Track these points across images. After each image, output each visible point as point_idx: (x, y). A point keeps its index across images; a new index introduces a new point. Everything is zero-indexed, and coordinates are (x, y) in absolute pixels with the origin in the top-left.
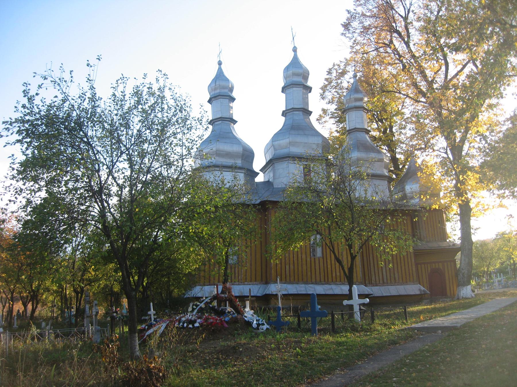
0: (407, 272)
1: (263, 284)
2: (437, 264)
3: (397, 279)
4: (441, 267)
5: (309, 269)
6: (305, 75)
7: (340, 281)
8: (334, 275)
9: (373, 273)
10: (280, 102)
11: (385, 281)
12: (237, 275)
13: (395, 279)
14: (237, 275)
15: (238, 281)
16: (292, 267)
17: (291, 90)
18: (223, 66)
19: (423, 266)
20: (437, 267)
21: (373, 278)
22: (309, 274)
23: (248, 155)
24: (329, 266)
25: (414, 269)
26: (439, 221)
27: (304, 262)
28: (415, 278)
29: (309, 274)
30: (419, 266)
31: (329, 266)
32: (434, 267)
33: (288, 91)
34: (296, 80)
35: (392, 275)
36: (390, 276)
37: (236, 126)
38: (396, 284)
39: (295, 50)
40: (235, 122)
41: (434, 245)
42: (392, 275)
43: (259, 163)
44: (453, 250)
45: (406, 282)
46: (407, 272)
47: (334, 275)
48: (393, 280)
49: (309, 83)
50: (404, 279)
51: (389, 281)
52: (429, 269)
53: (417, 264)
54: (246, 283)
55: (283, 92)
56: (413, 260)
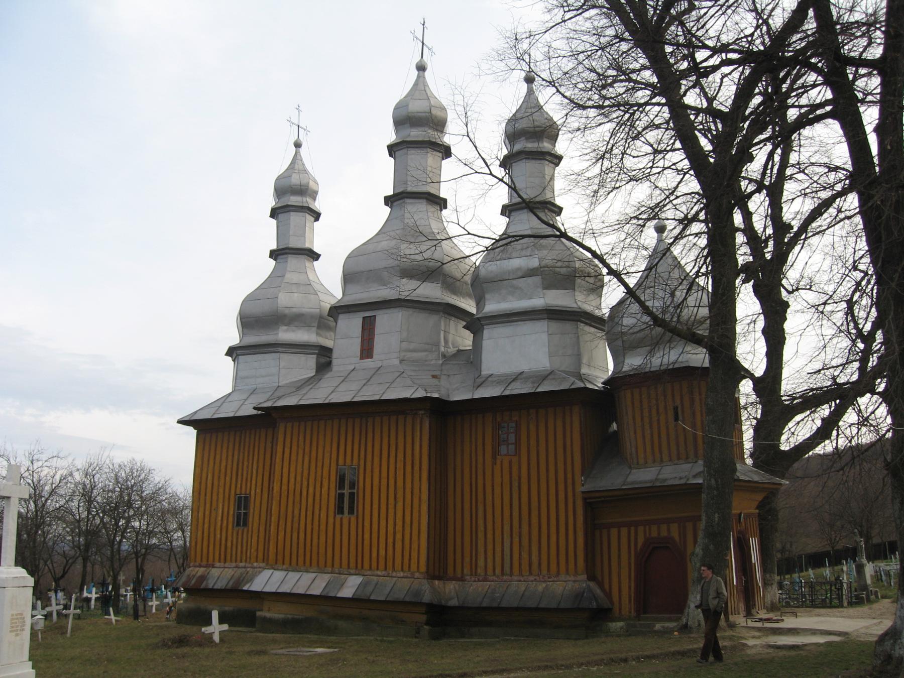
2: (664, 527)
3: (535, 566)
4: (675, 534)
5: (330, 541)
7: (386, 569)
8: (374, 555)
12: (244, 548)
13: (530, 565)
14: (244, 548)
15: (246, 561)
18: (303, 150)
19: (624, 531)
20: (664, 533)
21: (481, 563)
24: (367, 536)
26: (676, 409)
31: (367, 536)
32: (654, 534)
34: (419, 133)
35: (525, 555)
36: (520, 559)
38: (532, 578)
39: (421, 68)
42: (525, 555)
45: (558, 573)
47: (374, 555)
48: (525, 566)
50: (553, 566)
52: (641, 541)
54: (255, 564)
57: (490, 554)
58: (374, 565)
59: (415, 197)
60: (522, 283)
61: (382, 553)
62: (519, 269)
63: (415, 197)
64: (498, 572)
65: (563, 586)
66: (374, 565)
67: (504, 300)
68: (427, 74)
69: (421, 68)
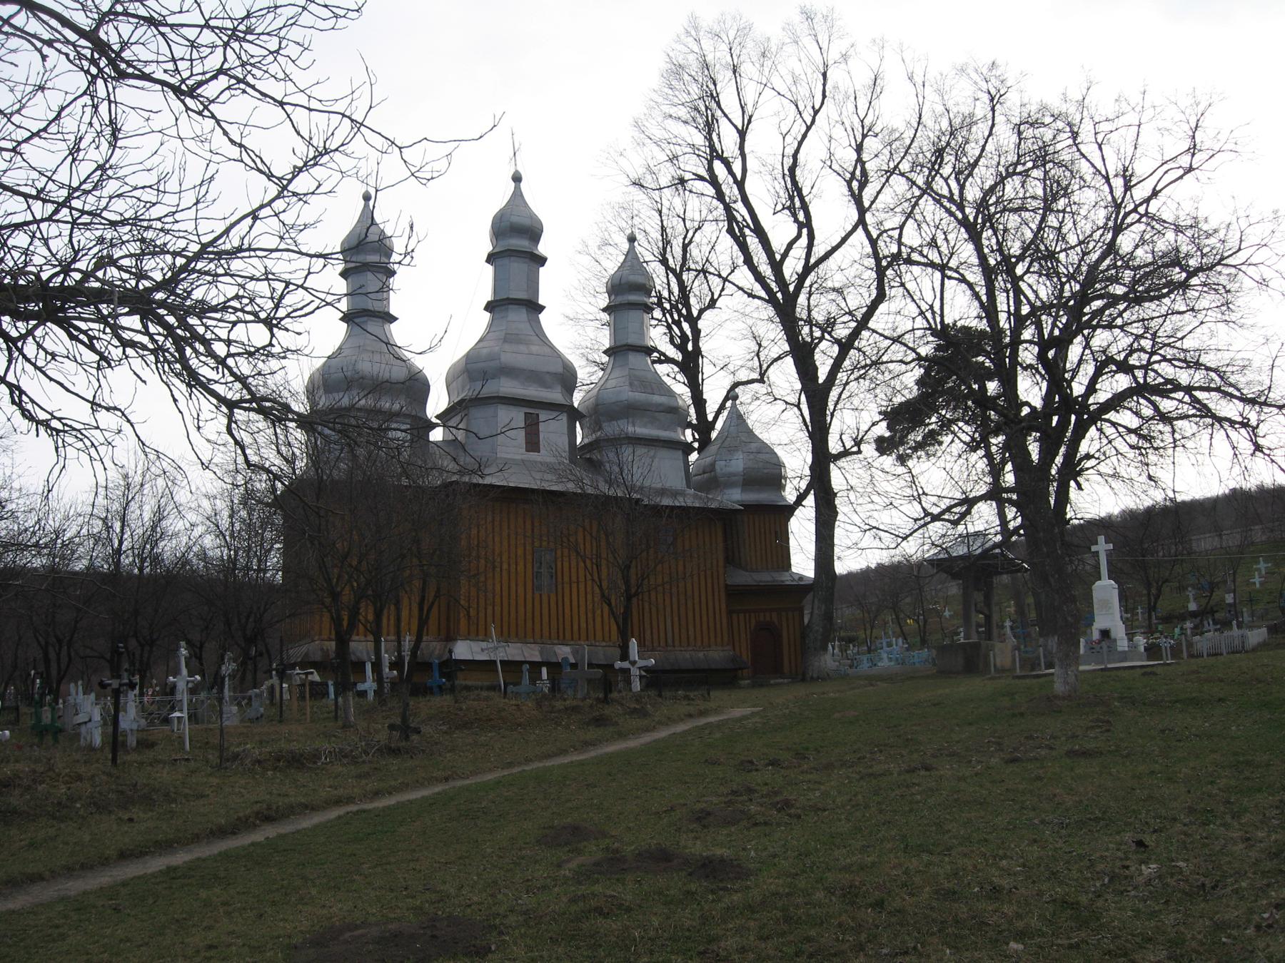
0: (711, 625)
1: (441, 640)
3: (692, 638)
5: (529, 615)
6: (533, 232)
8: (576, 627)
9: (647, 626)
10: (483, 283)
11: (670, 641)
16: (498, 609)
17: (506, 261)
19: (741, 616)
22: (529, 624)
23: (417, 387)
24: (567, 611)
25: (725, 621)
27: (521, 601)
28: (726, 639)
29: (529, 624)
30: (735, 616)
31: (567, 611)
33: (499, 262)
34: (516, 243)
37: (394, 327)
39: (517, 179)
40: (393, 319)
41: (765, 578)
43: (437, 402)
44: (801, 589)
46: (711, 625)
47: (576, 627)
49: (542, 248)
51: (677, 643)
52: (753, 621)
53: (730, 613)
55: (488, 261)
56: (724, 606)
57: (655, 631)
58: (576, 636)
59: (515, 302)
60: (662, 416)
61: (583, 625)
62: (661, 405)
63: (515, 302)
64: (662, 643)
65: (717, 655)
66: (576, 636)
67: (645, 426)
68: (522, 185)
69: (517, 179)
